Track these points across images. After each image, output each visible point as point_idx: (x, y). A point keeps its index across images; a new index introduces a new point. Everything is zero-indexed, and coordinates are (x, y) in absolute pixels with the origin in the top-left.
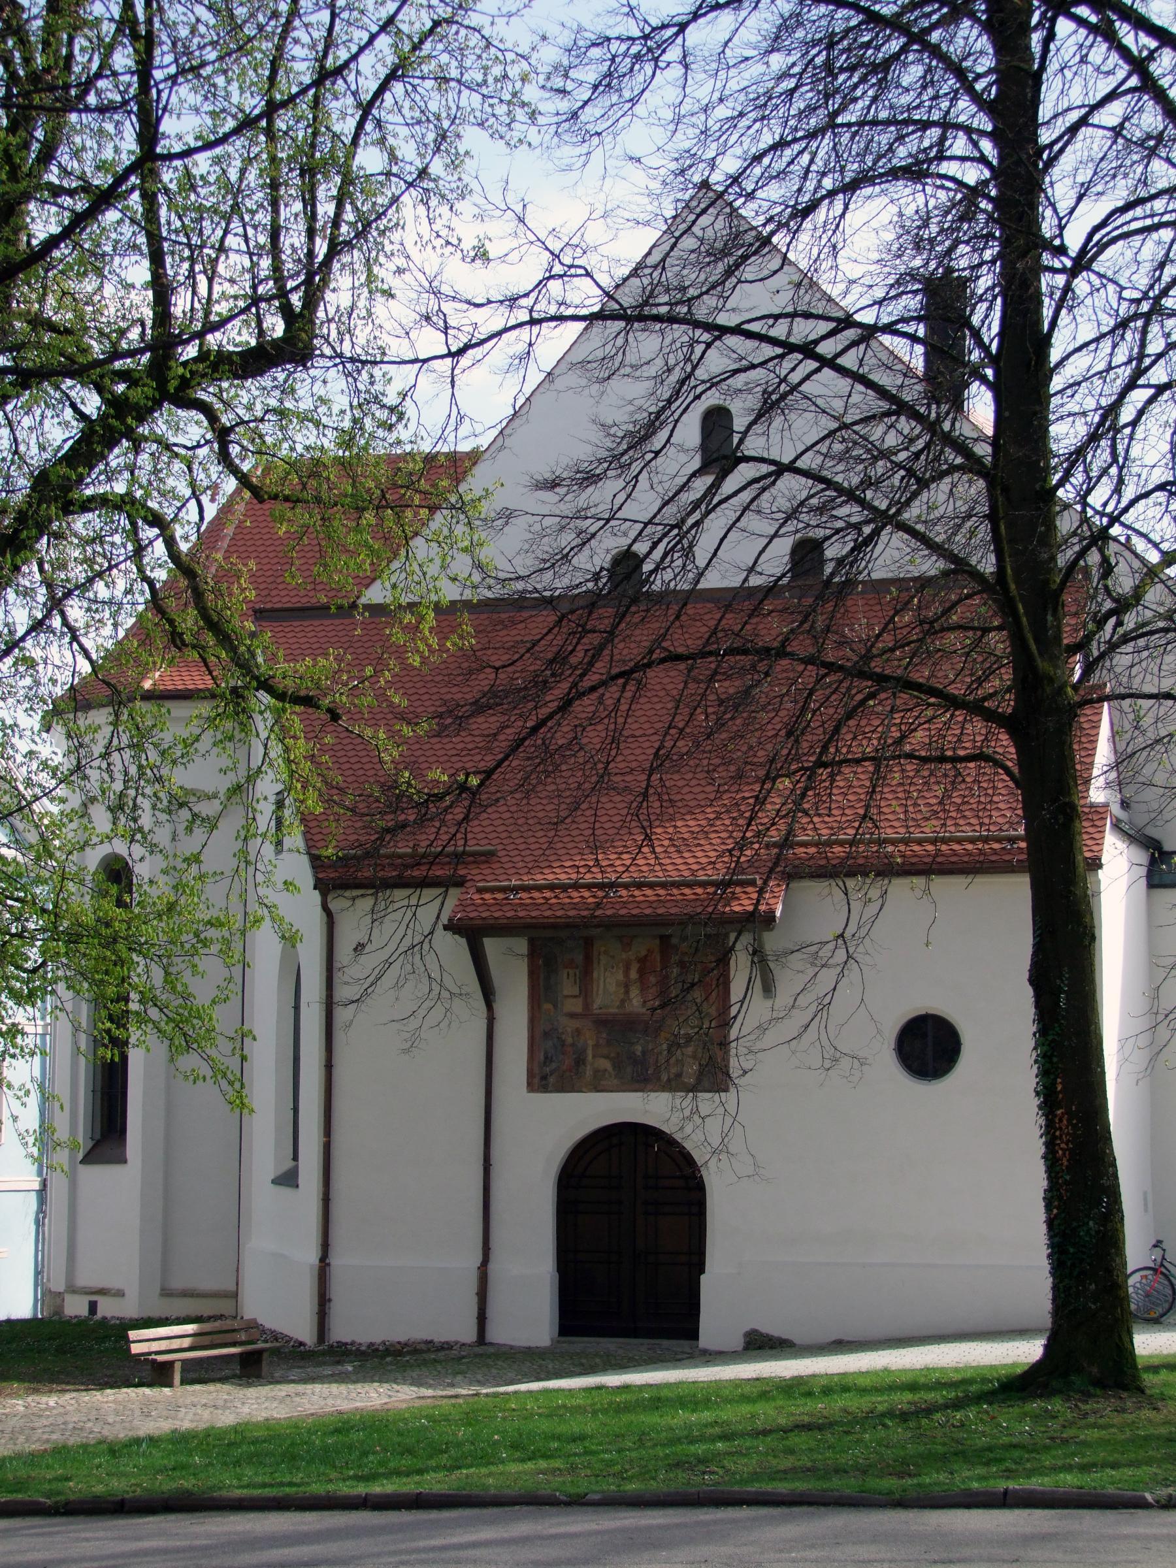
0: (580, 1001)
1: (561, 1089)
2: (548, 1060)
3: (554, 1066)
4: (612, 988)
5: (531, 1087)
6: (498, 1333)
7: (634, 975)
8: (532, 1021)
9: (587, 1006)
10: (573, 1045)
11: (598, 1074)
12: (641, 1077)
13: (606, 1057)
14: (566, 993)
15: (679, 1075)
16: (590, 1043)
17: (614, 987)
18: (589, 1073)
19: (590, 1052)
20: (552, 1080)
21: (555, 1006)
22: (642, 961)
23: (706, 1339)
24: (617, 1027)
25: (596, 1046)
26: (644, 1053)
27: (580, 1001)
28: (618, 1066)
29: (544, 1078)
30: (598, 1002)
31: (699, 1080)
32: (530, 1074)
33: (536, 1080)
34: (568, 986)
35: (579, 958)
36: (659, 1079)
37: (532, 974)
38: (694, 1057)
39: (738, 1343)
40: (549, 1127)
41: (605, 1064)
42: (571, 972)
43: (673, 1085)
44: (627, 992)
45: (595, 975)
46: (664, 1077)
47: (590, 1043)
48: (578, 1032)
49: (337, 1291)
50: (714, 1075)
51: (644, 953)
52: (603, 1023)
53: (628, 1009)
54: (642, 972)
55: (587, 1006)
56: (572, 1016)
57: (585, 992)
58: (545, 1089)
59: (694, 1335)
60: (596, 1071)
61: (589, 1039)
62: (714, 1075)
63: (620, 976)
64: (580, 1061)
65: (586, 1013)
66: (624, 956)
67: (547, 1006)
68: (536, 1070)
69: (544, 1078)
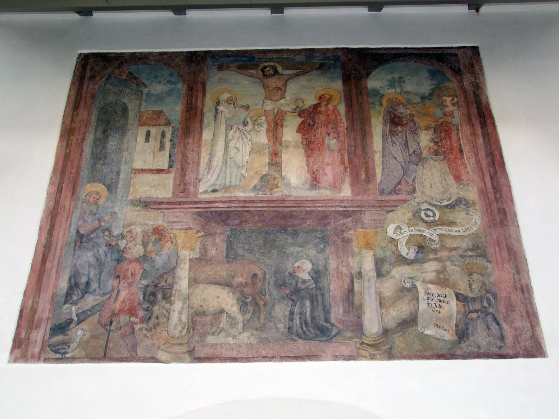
0: (170, 179)
2: (77, 288)
3: (90, 301)
7: (290, 134)
8: (53, 215)
9: (182, 186)
10: (145, 258)
13: (227, 284)
14: (138, 165)
15: (409, 323)
16: (186, 255)
18: (177, 313)
19: (183, 274)
20: (78, 333)
21: (111, 188)
24: (257, 225)
25: (203, 259)
26: (318, 274)
27: (170, 179)
28: (252, 301)
31: (462, 334)
32: (27, 319)
33: (39, 336)
35: (175, 110)
36: (358, 328)
37: (68, 132)
38: (442, 280)
42: (153, 130)
44: (275, 160)
45: (207, 135)
46: (372, 324)
47: (186, 255)
51: (310, 101)
52: (219, 217)
53: (277, 194)
56: (147, 204)
57: (182, 165)
63: (262, 138)
64: (157, 292)
66: (269, 106)
67: (90, 188)
68: (44, 307)
69: (61, 328)
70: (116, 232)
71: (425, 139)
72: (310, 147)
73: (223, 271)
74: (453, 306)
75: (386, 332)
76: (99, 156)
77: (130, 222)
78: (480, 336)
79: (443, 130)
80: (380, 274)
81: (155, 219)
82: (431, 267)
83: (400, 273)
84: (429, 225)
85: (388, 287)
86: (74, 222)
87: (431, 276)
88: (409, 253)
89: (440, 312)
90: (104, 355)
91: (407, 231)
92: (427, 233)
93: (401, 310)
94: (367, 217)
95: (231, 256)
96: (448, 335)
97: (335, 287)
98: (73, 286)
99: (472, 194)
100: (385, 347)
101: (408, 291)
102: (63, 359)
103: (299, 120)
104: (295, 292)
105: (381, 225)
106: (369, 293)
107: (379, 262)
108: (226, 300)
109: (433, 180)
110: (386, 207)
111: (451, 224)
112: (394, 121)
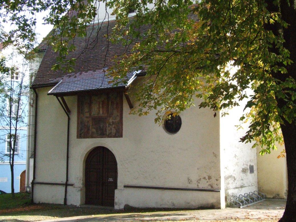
1: (84, 138)
2: (81, 130)
3: (83, 131)
4: (96, 109)
6: (69, 203)
7: (101, 106)
9: (90, 114)
11: (93, 133)
12: (103, 134)
15: (111, 133)
17: (97, 110)
20: (82, 135)
22: (103, 102)
23: (116, 207)
24: (97, 120)
25: (93, 125)
29: (81, 134)
31: (115, 134)
33: (79, 135)
34: (86, 110)
36: (106, 134)
37: (78, 107)
38: (114, 128)
40: (83, 147)
41: (94, 130)
43: (110, 136)
44: (99, 111)
45: (92, 106)
46: (108, 134)
48: (88, 122)
50: (119, 134)
54: (102, 105)
55: (90, 114)
56: (87, 117)
57: (90, 112)
61: (90, 124)
62: (119, 134)
63: (98, 106)
64: (89, 129)
67: (81, 115)
69: (81, 134)
70: (84, 122)
71: (115, 106)
72: (103, 107)
74: (115, 131)
75: (109, 134)
77: (85, 119)
78: (117, 135)
79: (117, 104)
80: (109, 127)
82: (114, 126)
83: (111, 126)
84: (114, 120)
85: (109, 128)
87: (113, 127)
88: (112, 124)
89: (114, 131)
91: (112, 121)
92: (114, 121)
93: (110, 132)
94: (108, 119)
96: (114, 135)
98: (81, 129)
99: (119, 114)
101: (111, 129)
102: (81, 138)
103: (102, 103)
105: (109, 120)
106: (108, 129)
107: (109, 124)
109: (116, 113)
110: (110, 117)
111: (116, 119)
112: (112, 102)
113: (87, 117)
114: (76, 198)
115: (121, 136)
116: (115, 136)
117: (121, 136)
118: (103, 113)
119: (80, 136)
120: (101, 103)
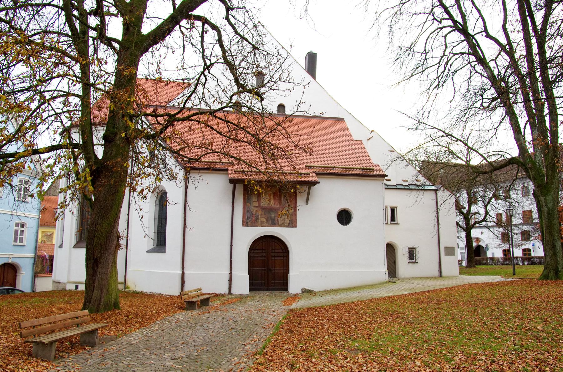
5: (243, 225)
7: (272, 197)
9: (259, 204)
11: (261, 221)
12: (274, 223)
15: (283, 223)
18: (259, 222)
20: (249, 223)
24: (268, 210)
25: (262, 215)
26: (274, 217)
28: (267, 220)
30: (262, 204)
32: (243, 221)
39: (299, 292)
40: (248, 235)
41: (264, 220)
46: (280, 223)
49: (185, 279)
50: (292, 224)
52: (263, 209)
54: (274, 196)
55: (259, 204)
56: (255, 207)
57: (259, 201)
58: (247, 226)
59: (287, 290)
60: (261, 221)
61: (260, 213)
62: (292, 224)
65: (259, 206)
67: (248, 204)
69: (247, 223)
72: (274, 199)
73: (264, 216)
76: (248, 199)
77: (254, 209)
81: (256, 209)
86: (247, 209)
90: (252, 226)
95: (265, 214)
97: (276, 218)
100: (281, 226)
101: (284, 219)
104: (272, 219)
108: (264, 220)
113: (255, 207)
114: (242, 284)
115: (295, 226)
116: (288, 226)
117: (295, 226)
118: (274, 204)
119: (246, 223)
120: (272, 195)
